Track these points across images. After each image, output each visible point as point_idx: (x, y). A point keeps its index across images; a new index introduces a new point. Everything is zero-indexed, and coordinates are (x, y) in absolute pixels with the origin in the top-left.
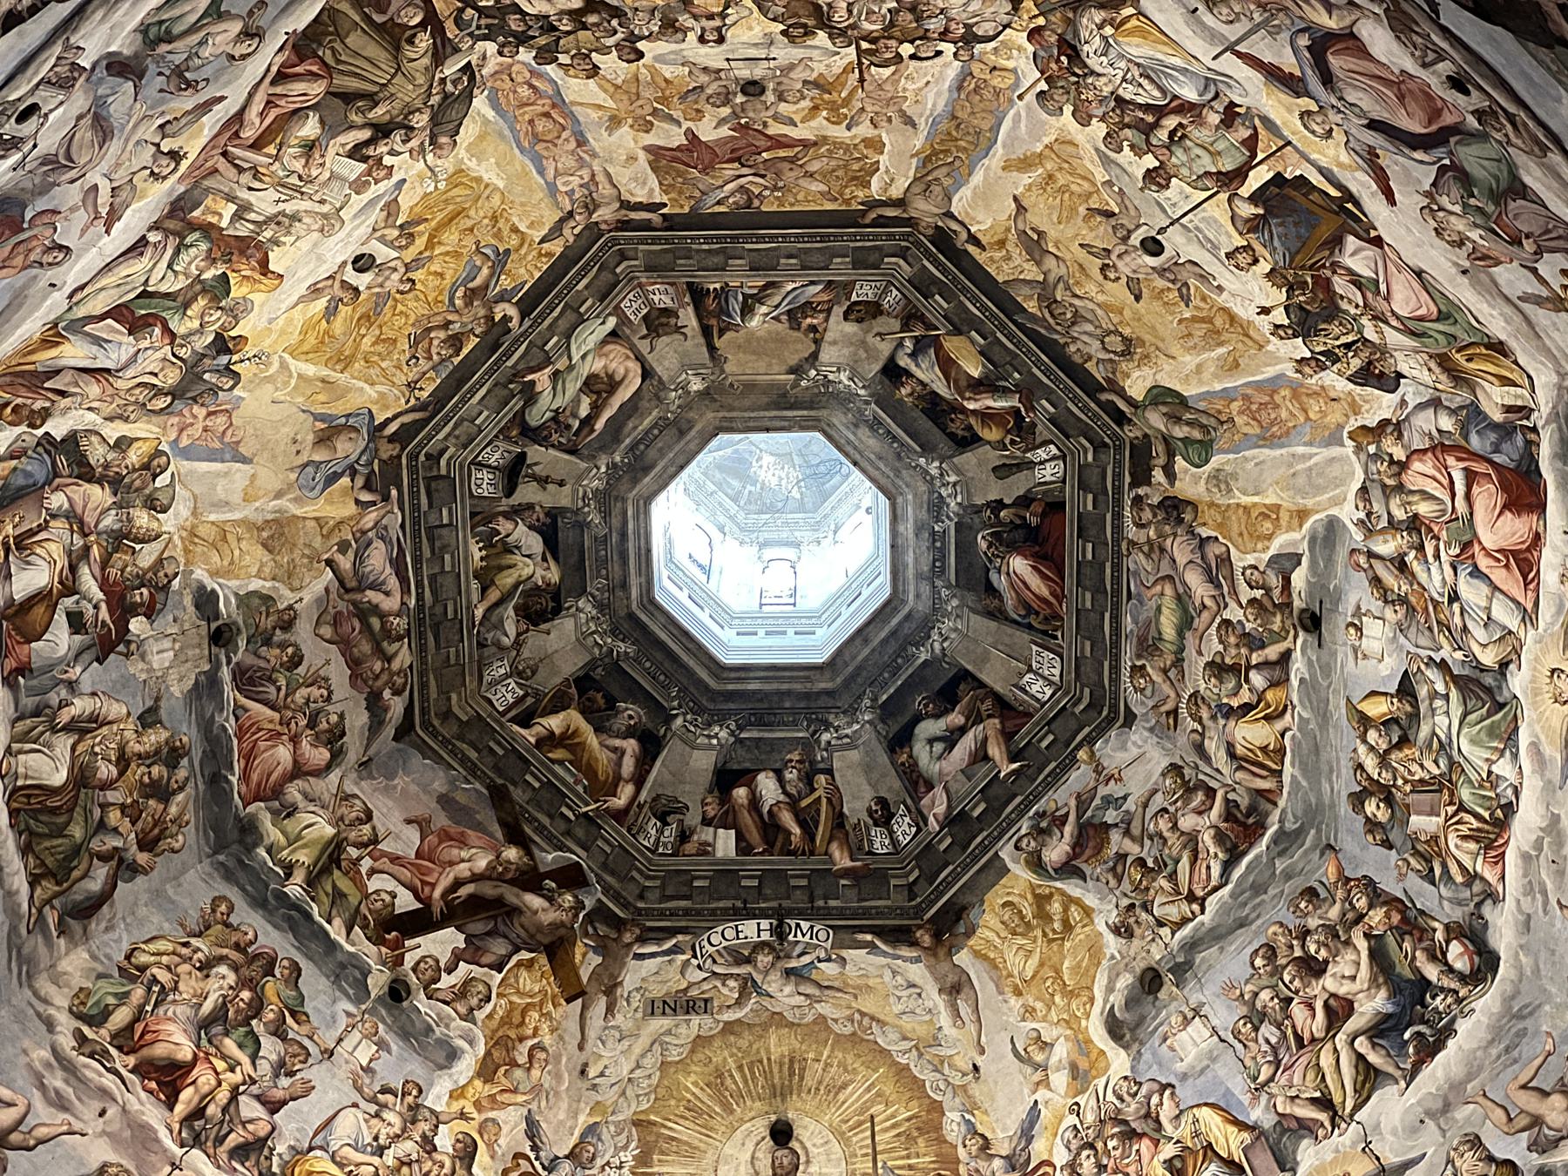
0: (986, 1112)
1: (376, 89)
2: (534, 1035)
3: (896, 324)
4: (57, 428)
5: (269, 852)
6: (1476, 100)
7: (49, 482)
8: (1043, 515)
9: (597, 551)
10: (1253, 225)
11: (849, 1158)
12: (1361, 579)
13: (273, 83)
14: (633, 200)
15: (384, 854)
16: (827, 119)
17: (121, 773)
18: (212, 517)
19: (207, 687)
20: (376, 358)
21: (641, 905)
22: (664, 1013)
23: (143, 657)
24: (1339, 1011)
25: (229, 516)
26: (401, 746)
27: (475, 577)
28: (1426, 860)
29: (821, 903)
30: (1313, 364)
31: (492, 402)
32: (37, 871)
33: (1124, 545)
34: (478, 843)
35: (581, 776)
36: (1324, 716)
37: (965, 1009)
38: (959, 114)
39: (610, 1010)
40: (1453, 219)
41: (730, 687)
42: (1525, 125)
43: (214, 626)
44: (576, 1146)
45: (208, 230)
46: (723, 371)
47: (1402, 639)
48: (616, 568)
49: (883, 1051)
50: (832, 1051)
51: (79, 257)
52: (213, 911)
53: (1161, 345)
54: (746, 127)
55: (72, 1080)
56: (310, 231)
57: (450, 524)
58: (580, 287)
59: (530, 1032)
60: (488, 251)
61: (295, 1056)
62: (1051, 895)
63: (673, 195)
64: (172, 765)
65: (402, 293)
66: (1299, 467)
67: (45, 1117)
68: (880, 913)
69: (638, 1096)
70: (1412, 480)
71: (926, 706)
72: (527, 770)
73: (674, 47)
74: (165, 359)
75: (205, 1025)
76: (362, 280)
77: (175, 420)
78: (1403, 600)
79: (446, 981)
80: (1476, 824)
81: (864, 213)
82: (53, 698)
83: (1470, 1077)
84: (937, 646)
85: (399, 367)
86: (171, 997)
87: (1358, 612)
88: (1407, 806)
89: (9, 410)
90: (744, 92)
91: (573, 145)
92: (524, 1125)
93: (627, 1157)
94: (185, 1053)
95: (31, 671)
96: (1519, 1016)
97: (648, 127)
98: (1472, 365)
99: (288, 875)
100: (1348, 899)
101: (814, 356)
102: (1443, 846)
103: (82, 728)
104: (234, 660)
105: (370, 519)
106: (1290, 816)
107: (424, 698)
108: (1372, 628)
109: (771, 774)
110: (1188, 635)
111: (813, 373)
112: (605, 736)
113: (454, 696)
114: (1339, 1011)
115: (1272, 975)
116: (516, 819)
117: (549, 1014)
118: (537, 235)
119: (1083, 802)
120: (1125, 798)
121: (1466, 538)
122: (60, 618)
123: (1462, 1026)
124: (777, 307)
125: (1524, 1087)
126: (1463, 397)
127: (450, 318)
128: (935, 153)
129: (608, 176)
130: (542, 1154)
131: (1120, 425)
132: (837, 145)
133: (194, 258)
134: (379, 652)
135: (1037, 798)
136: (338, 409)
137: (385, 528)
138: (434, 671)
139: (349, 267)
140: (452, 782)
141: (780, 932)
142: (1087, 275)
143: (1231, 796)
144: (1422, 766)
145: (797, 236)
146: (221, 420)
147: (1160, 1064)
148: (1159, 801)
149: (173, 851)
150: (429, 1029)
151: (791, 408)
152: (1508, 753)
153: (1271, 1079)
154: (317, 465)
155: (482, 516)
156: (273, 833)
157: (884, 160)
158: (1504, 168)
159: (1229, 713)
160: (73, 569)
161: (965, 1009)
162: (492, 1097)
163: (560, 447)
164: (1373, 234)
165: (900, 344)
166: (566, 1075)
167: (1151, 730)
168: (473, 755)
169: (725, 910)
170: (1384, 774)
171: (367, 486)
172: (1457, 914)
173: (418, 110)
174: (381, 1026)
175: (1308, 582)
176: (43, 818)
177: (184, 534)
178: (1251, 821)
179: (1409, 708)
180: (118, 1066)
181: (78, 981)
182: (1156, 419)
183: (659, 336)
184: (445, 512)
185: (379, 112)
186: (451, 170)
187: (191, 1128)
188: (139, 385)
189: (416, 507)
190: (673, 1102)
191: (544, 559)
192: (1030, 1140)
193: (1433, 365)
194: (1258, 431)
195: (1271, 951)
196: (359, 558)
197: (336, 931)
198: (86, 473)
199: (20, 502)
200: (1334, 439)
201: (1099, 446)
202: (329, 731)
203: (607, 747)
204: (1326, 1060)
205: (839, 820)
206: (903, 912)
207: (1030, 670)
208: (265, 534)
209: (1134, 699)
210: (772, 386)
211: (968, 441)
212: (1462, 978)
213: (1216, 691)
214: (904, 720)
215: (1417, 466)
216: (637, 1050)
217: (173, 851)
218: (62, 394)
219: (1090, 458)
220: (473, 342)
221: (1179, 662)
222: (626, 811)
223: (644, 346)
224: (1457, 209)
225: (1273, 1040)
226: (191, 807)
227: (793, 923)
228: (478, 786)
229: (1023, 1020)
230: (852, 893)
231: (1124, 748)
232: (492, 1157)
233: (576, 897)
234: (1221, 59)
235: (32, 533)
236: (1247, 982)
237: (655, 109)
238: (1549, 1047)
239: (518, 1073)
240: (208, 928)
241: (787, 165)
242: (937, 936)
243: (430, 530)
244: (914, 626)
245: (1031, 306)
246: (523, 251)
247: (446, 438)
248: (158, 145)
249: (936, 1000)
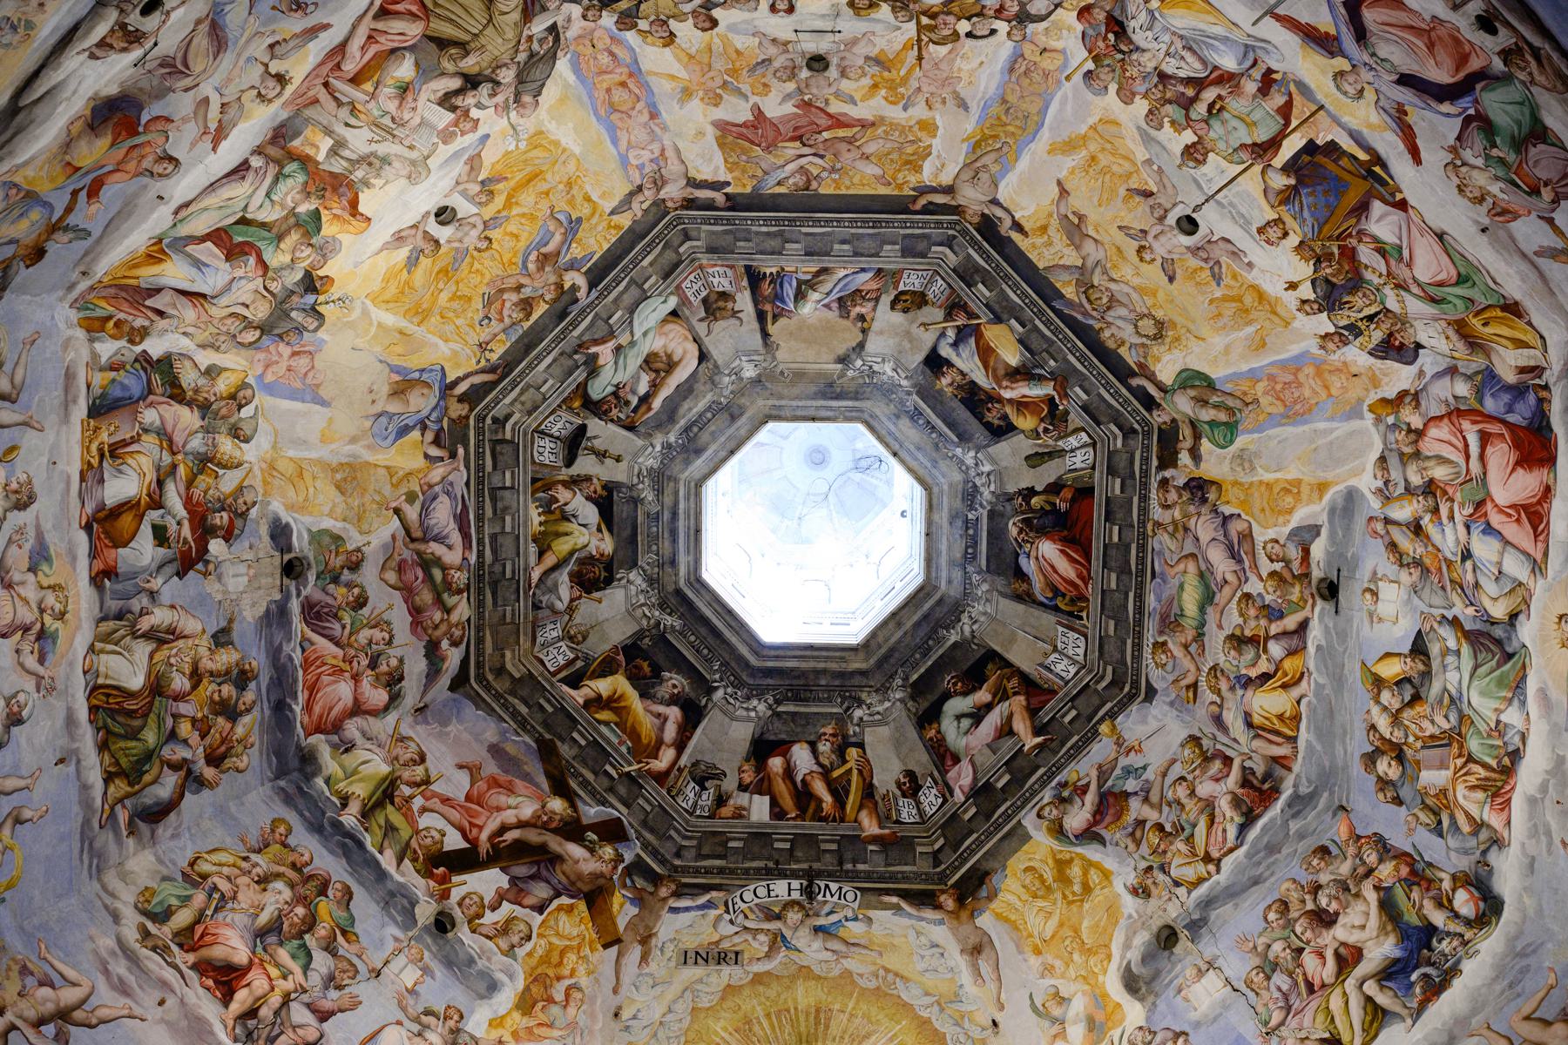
1: (467, 38)
2: (572, 975)
3: (939, 314)
4: (155, 347)
5: (327, 781)
6: (1504, 39)
7: (143, 398)
8: (1073, 501)
10: (1287, 197)
12: (1378, 546)
13: (376, 17)
14: (699, 177)
15: (435, 795)
16: (886, 99)
17: (195, 687)
18: (291, 453)
19: (276, 616)
20: (451, 315)
21: (677, 862)
23: (219, 578)
24: (1348, 958)
25: (306, 454)
26: (456, 696)
27: (534, 541)
28: (1435, 813)
29: (849, 866)
30: (1336, 339)
31: (557, 370)
32: (112, 769)
33: (1150, 527)
34: (523, 791)
36: (1338, 680)
37: (985, 967)
38: (1010, 98)
39: (645, 958)
40: (1475, 173)
41: (770, 664)
42: (1549, 58)
43: (287, 557)
45: (305, 161)
46: (774, 358)
47: (1416, 600)
48: (667, 543)
49: (905, 1005)
50: (857, 1002)
51: (187, 171)
52: (273, 831)
53: (1192, 327)
54: (806, 105)
55: (135, 968)
56: (398, 176)
57: (512, 488)
58: (645, 263)
59: (567, 972)
60: (561, 217)
61: (344, 972)
62: (1071, 861)
63: (736, 174)
64: (241, 685)
65: (479, 250)
66: (1320, 442)
67: (107, 1000)
68: (905, 878)
69: (668, 1038)
70: (1429, 446)
71: (955, 684)
72: (574, 728)
73: (746, 15)
74: (256, 291)
75: (261, 934)
76: (443, 233)
77: (261, 356)
78: (1418, 563)
79: (490, 918)
80: (1483, 773)
81: (915, 199)
82: (136, 604)
83: (1474, 1012)
84: (967, 629)
85: (472, 326)
86: (230, 905)
87: (1374, 577)
88: (1418, 763)
89: (111, 324)
90: (809, 67)
91: (646, 117)
94: (241, 956)
95: (117, 575)
96: (1523, 954)
97: (716, 100)
98: (1489, 330)
99: (344, 806)
100: (1359, 855)
101: (861, 346)
102: (1451, 797)
103: (162, 637)
104: (304, 593)
105: (437, 473)
106: (1304, 780)
107: (480, 652)
108: (1388, 592)
109: (805, 746)
110: (1209, 610)
111: (859, 363)
112: (649, 702)
113: (508, 654)
114: (1348, 958)
115: (1284, 928)
116: (563, 774)
117: (585, 958)
118: (608, 206)
119: (1103, 773)
120: (1145, 768)
121: (1479, 498)
122: (146, 531)
123: (1467, 966)
124: (828, 294)
125: (1527, 1018)
126: (1479, 362)
127: (524, 281)
128: (984, 139)
129: (678, 151)
131: (1149, 410)
132: (894, 126)
133: (290, 191)
134: (439, 602)
135: (1060, 768)
136: (414, 362)
137: (451, 484)
138: (491, 626)
139: (432, 218)
140: (503, 733)
141: (809, 892)
142: (1124, 258)
143: (1248, 764)
144: (1432, 722)
145: (851, 221)
146: (302, 363)
147: (1174, 1015)
148: (1177, 770)
149: (238, 770)
150: (471, 961)
151: (838, 397)
152: (1516, 702)
153: (1282, 1023)
154: (391, 416)
155: (542, 484)
156: (329, 762)
157: (936, 143)
158: (1527, 111)
159: (1247, 683)
160: (160, 483)
161: (985, 967)
162: (529, 1030)
163: (618, 422)
164: (1399, 197)
165: (943, 335)
166: (600, 1017)
167: (1172, 704)
168: (524, 710)
169: (758, 870)
170: (1396, 733)
171: (437, 442)
172: (1463, 863)
173: (505, 65)
174: (427, 954)
175: (1328, 553)
176: (120, 719)
177: (264, 466)
178: (1266, 786)
179: (1421, 667)
180: (178, 961)
181: (145, 880)
182: (1183, 405)
183: (716, 319)
184: (508, 475)
185: (470, 63)
186: (532, 131)
187: (245, 1026)
188: (232, 315)
189: (480, 468)
191: (599, 530)
193: (1451, 333)
194: (1282, 409)
195: (1284, 906)
196: (425, 510)
197: (387, 861)
198: (177, 394)
199: (116, 412)
200: (1354, 413)
201: (1128, 432)
202: (390, 674)
204: (1336, 1003)
205: (869, 791)
206: (928, 878)
207: (1055, 649)
208: (338, 476)
209: (1157, 677)
210: (820, 374)
211: (1002, 430)
212: (1468, 923)
213: (1235, 663)
214: (932, 698)
215: (1433, 432)
216: (669, 996)
217: (238, 770)
218: (161, 313)
219: (1119, 443)
220: (540, 310)
221: (1200, 636)
222: (668, 772)
223: (701, 329)
224: (1480, 162)
225: (1285, 988)
226: (256, 728)
227: (822, 884)
228: (528, 739)
229: (1043, 976)
230: (880, 859)
231: (1144, 721)
234: (1260, 24)
235: (125, 443)
236: (1260, 935)
237: (725, 83)
238: (1551, 981)
239: (555, 1010)
240: (267, 846)
241: (843, 146)
242: (961, 900)
243: (493, 490)
244: (945, 609)
245: (1069, 292)
246: (594, 221)
247: (512, 403)
248: (266, 65)
249: (961, 962)
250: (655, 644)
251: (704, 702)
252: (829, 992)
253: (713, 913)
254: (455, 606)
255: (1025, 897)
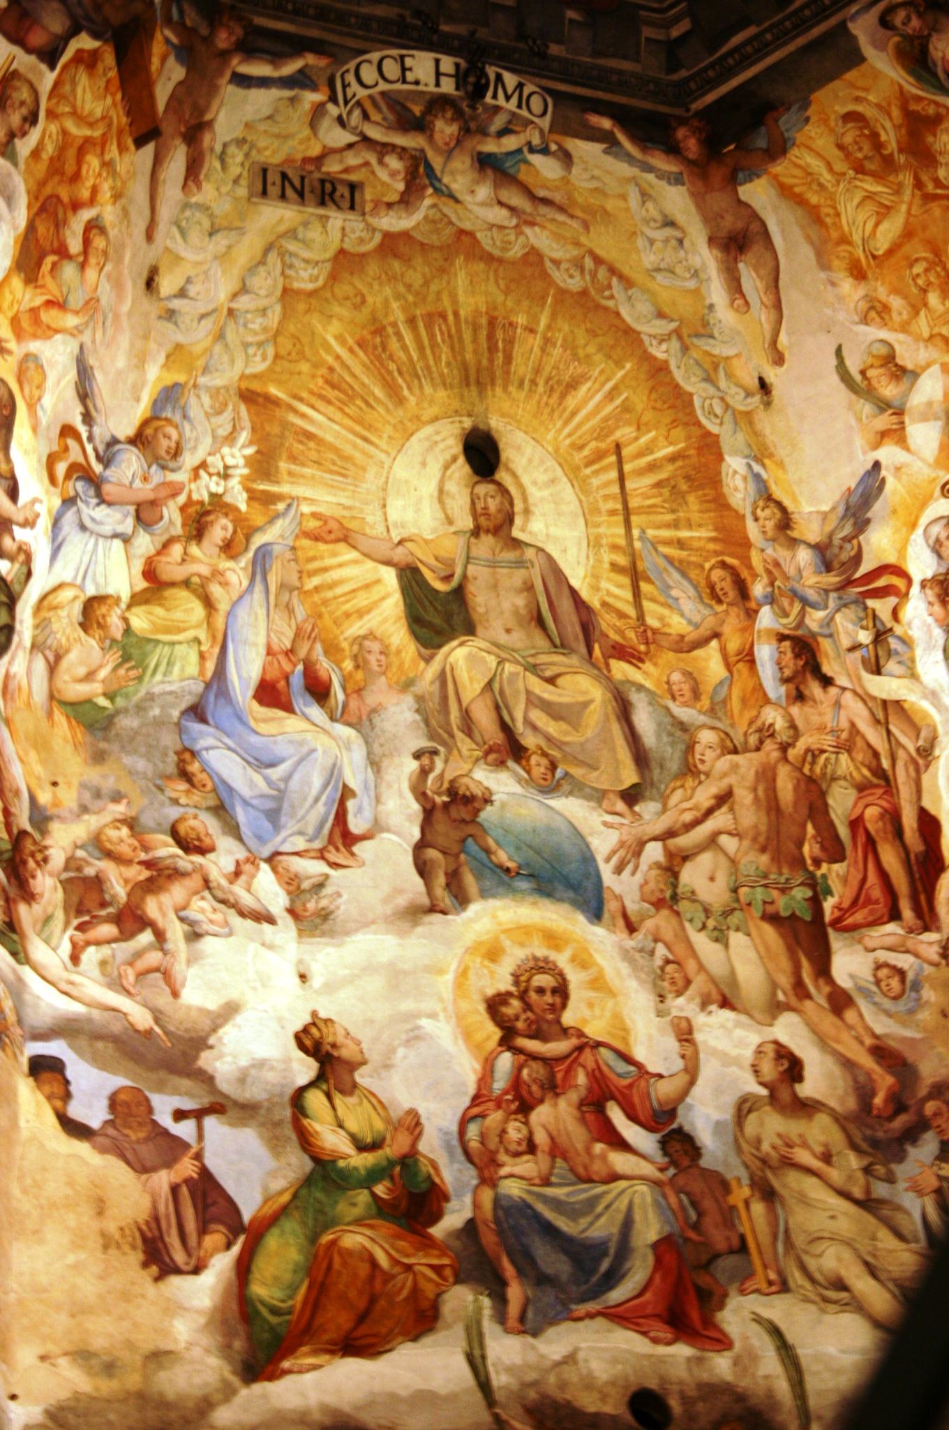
0: (781, 465)
2: (92, 201)
11: (589, 514)
22: (283, 197)
37: (751, 281)
39: (193, 171)
44: (145, 423)
49: (629, 332)
50: (553, 316)
59: (85, 194)
68: (623, 83)
69: (246, 345)
92: (72, 374)
93: (238, 455)
117: (107, 165)
130: (97, 430)
161: (751, 281)
162: (34, 311)
166: (129, 286)
190: (305, 367)
192: (862, 525)
227: (491, 71)
229: (865, 320)
232: (35, 429)
239: (69, 271)
242: (712, 146)
249: (706, 258)
252: (507, 292)
253: (311, 98)
255: (840, 166)
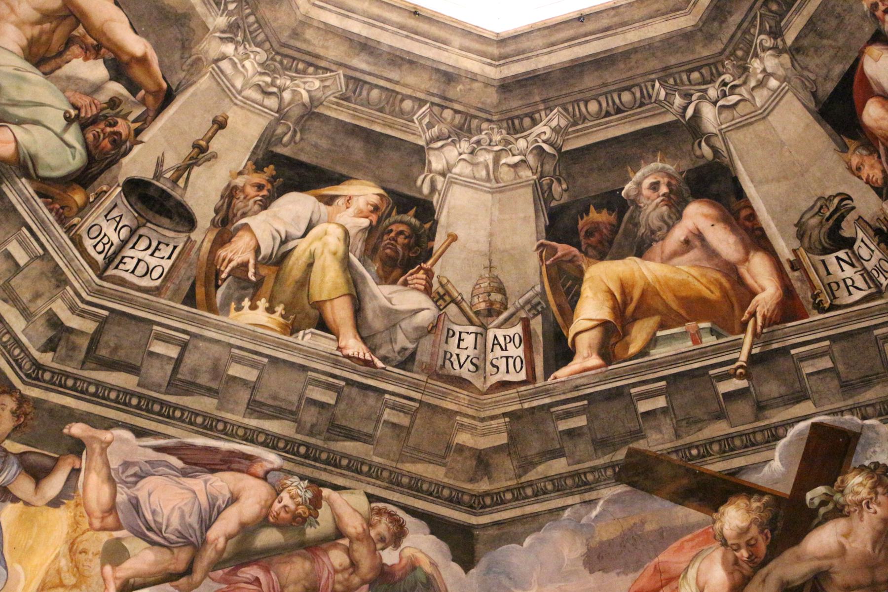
9: (368, 103)
27: (293, 330)
34: (684, 558)
35: (691, 325)
48: (411, 79)
72: (632, 402)
107: (434, 493)
109: (875, 50)
112: (657, 247)
113: (463, 438)
116: (690, 472)
140: (578, 528)
163: (145, 121)
168: (559, 466)
184: (158, 348)
191: (329, 201)
203: (675, 254)
222: (787, 290)
233: (862, 468)
243: (177, 385)
250: (570, 177)
251: (706, 151)
254: (336, 518)
